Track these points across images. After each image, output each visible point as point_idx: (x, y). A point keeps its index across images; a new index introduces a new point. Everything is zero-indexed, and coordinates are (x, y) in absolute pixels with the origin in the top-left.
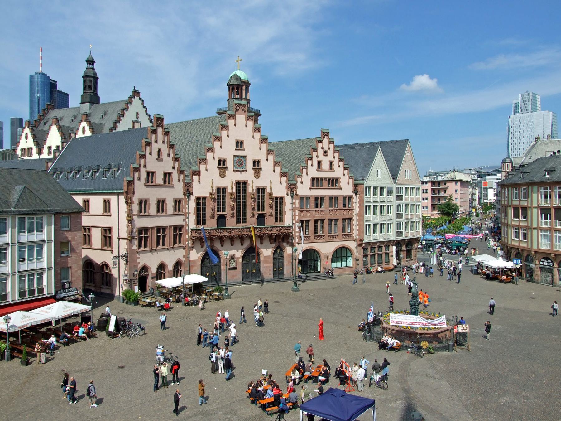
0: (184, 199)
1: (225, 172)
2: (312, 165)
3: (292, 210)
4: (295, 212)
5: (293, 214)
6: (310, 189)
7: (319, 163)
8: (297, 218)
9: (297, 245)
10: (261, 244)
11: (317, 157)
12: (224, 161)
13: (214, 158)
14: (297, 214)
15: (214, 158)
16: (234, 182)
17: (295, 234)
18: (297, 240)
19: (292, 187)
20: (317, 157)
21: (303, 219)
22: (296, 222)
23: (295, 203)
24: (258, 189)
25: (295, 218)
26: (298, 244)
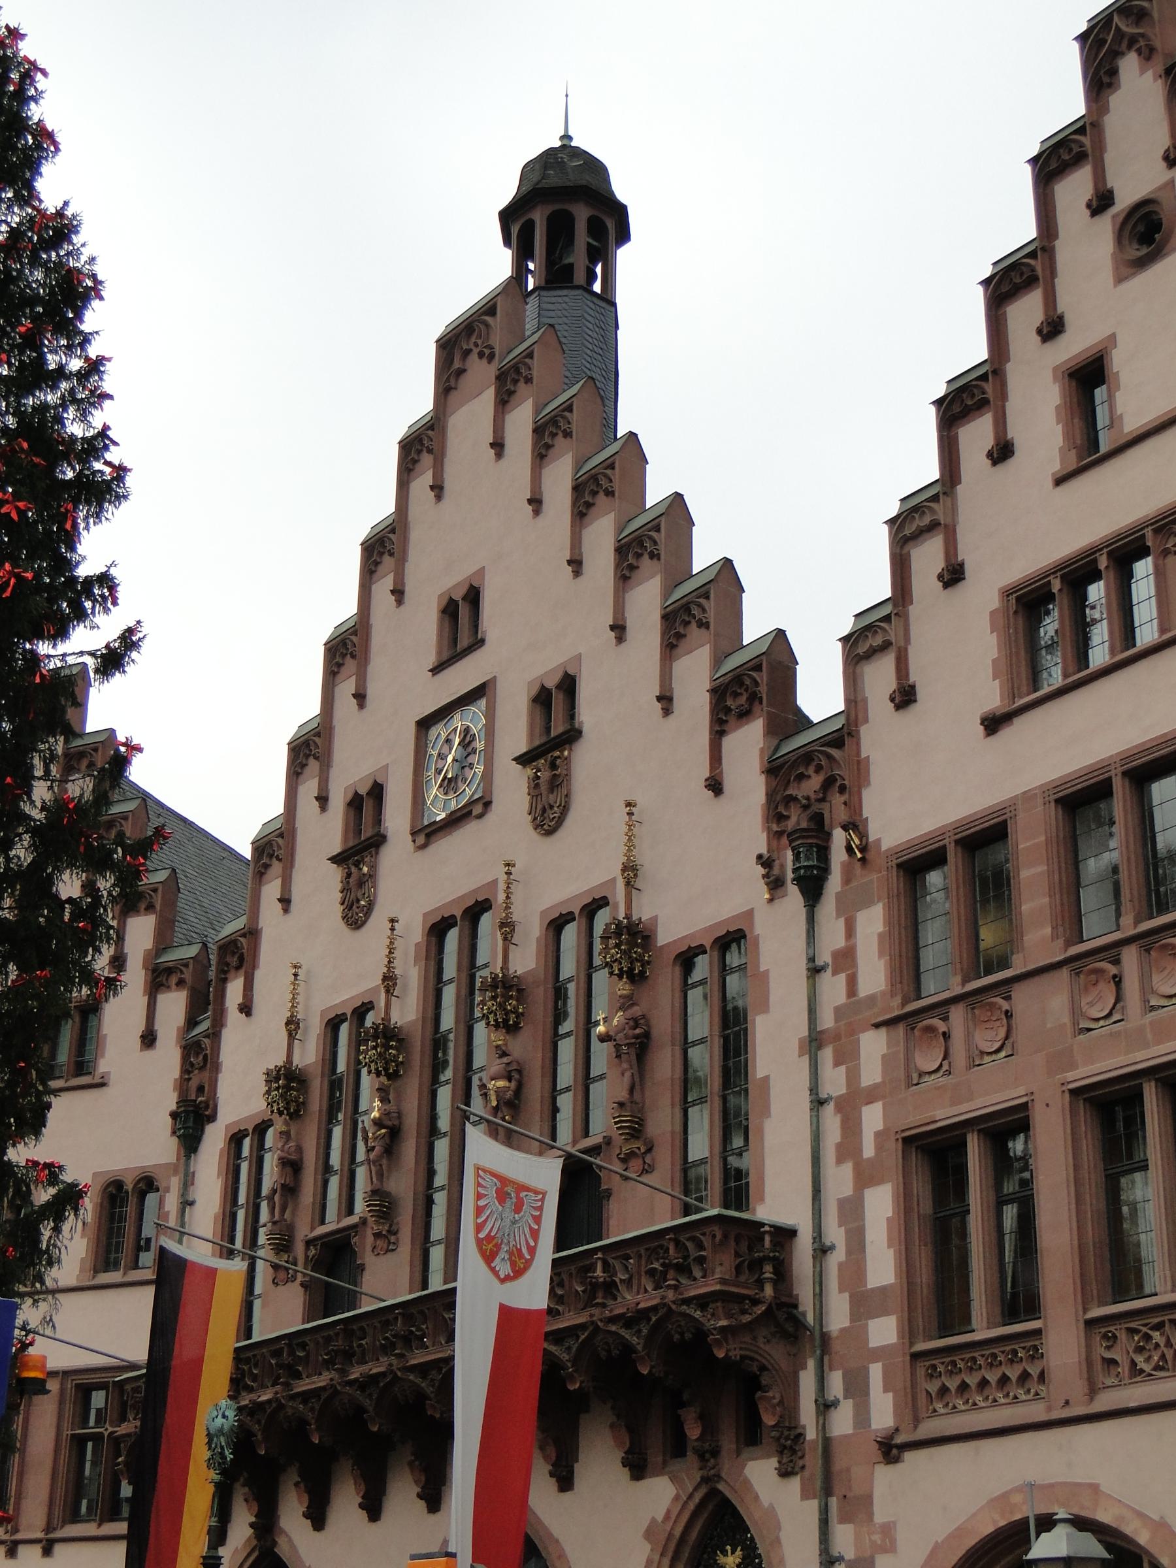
0: (175, 1169)
1: (372, 876)
2: (1002, 452)
3: (814, 1041)
4: (847, 1056)
5: (834, 1082)
6: (993, 724)
7: (1089, 377)
8: (873, 1118)
9: (884, 1479)
10: (565, 1482)
11: (1052, 328)
12: (377, 791)
13: (323, 800)
14: (871, 1074)
15: (323, 800)
16: (414, 933)
17: (856, 1332)
18: (883, 1413)
19: (813, 783)
20: (1052, 328)
21: (945, 1113)
22: (865, 1178)
23: (846, 959)
24: (557, 925)
25: (851, 1127)
26: (891, 1450)
